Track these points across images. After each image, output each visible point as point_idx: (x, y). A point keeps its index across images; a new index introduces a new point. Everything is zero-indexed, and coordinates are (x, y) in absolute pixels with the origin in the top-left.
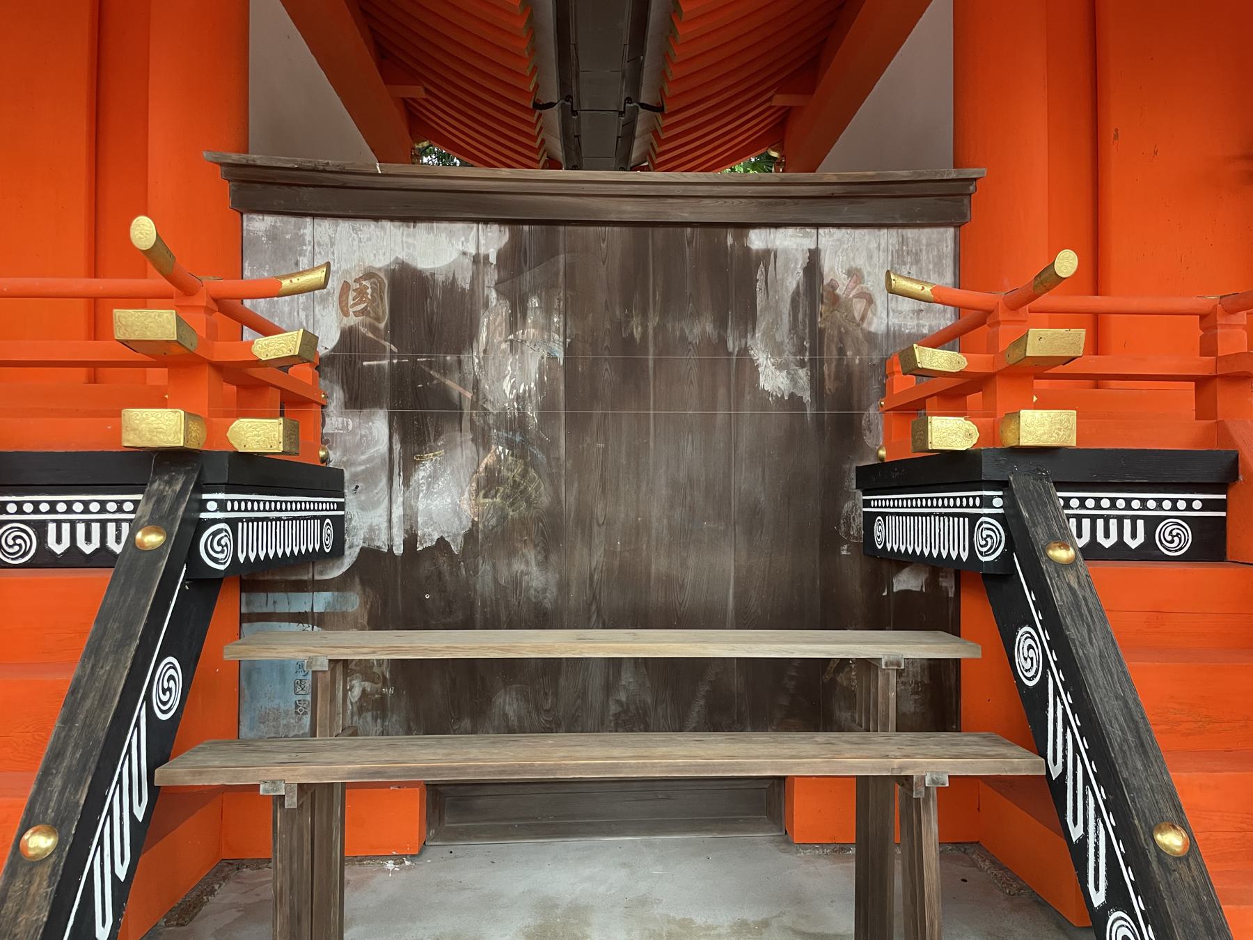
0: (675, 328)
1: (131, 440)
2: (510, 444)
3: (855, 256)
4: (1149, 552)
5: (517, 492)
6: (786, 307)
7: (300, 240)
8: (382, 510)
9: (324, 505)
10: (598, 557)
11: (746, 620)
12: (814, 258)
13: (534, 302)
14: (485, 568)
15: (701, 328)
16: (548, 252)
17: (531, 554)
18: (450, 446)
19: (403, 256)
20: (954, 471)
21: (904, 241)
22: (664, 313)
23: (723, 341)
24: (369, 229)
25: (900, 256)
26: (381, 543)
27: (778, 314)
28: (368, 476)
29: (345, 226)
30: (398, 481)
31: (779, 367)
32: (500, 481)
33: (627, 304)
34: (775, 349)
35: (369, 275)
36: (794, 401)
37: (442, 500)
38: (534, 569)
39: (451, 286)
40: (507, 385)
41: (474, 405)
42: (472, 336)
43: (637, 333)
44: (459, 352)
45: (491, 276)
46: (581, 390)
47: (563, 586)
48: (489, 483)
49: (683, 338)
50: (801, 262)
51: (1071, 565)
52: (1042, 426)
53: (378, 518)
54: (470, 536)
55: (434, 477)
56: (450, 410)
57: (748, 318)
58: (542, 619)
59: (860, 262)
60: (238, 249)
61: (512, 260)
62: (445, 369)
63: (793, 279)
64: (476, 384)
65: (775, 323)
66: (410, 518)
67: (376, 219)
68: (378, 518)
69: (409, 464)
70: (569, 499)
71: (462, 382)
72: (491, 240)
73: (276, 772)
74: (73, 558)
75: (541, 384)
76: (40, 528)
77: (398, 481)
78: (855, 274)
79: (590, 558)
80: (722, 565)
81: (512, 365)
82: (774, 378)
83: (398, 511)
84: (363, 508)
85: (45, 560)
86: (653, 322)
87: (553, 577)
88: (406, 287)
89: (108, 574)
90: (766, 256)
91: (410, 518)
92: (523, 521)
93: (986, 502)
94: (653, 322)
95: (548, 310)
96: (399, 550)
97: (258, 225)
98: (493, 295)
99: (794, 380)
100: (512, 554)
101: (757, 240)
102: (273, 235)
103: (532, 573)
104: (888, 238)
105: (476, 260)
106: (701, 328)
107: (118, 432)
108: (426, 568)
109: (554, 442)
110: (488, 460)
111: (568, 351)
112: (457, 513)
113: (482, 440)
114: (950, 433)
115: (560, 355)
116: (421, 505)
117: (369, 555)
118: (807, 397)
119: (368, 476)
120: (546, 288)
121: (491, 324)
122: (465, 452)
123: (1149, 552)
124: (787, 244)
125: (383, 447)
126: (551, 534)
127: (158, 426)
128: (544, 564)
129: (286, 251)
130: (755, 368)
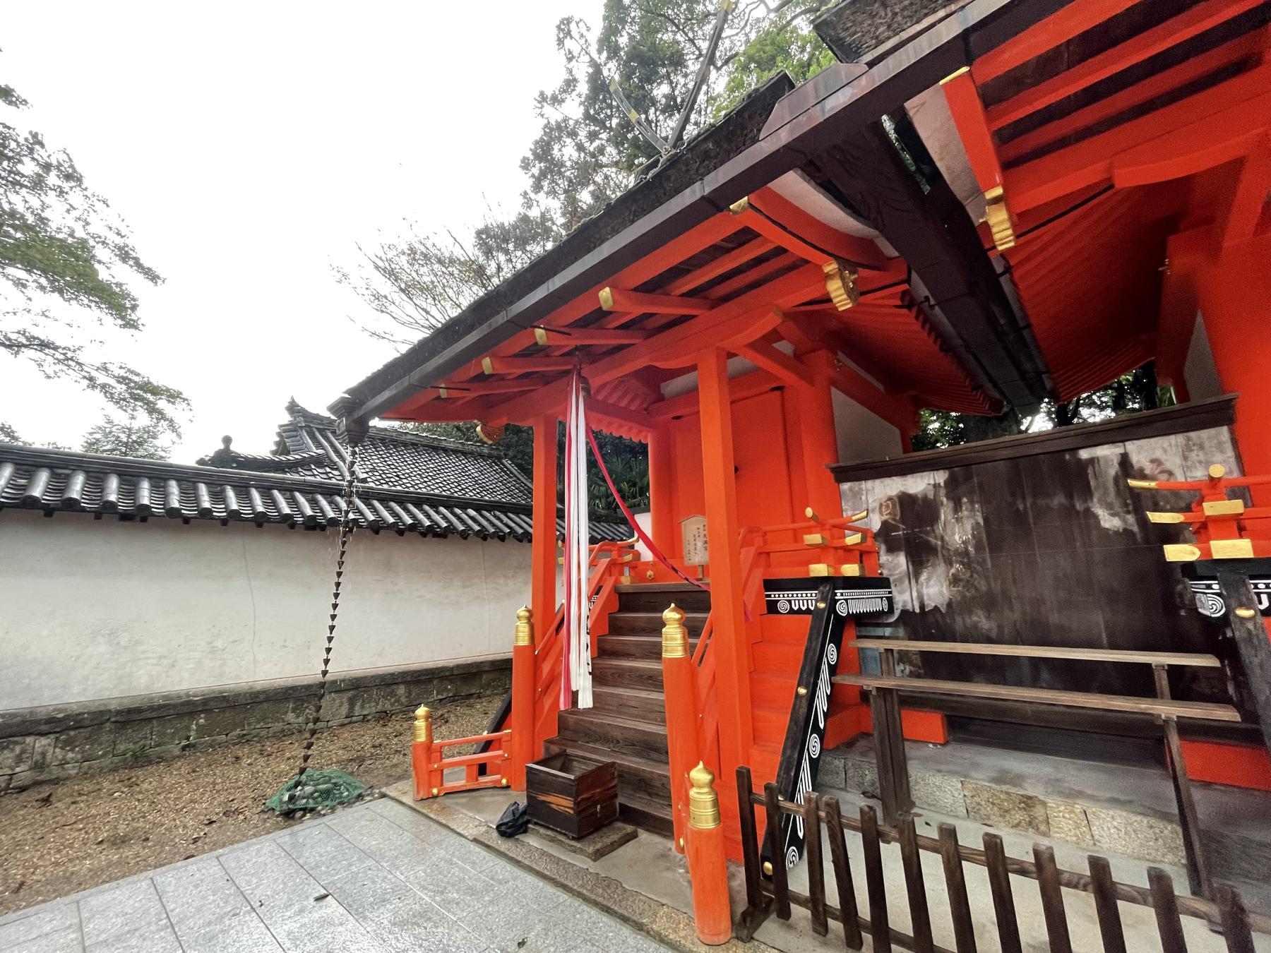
0: (1042, 502)
1: (812, 575)
2: (962, 563)
5: (969, 584)
6: (1111, 484)
7: (861, 489)
8: (908, 593)
9: (882, 592)
10: (1017, 615)
11: (1114, 646)
13: (965, 500)
14: (958, 619)
15: (1058, 500)
16: (968, 478)
17: (980, 613)
18: (934, 565)
19: (902, 489)
21: (1189, 439)
22: (1035, 496)
23: (1073, 506)
24: (887, 481)
25: (1188, 448)
26: (909, 607)
27: (1106, 488)
28: (900, 580)
29: (877, 482)
30: (913, 582)
31: (1113, 515)
32: (961, 580)
33: (1013, 494)
34: (1109, 507)
35: (890, 499)
36: (1127, 532)
37: (934, 589)
38: (984, 620)
39: (925, 498)
40: (957, 537)
41: (943, 547)
42: (937, 518)
43: (1021, 507)
44: (932, 526)
45: (942, 492)
46: (991, 538)
47: (1000, 627)
48: (955, 581)
49: (1048, 507)
51: (1252, 618)
53: (906, 597)
54: (949, 605)
55: (928, 579)
57: (1087, 493)
58: (989, 640)
59: (1158, 454)
60: (839, 496)
61: (951, 484)
62: (927, 533)
63: (1113, 470)
64: (942, 539)
65: (1106, 493)
66: (920, 597)
67: (890, 476)
68: (906, 597)
69: (917, 575)
70: (997, 588)
71: (936, 538)
72: (941, 477)
73: (868, 682)
74: (800, 611)
75: (973, 535)
76: (790, 602)
77: (913, 582)
79: (1013, 616)
80: (1098, 619)
81: (958, 529)
83: (915, 594)
84: (901, 593)
85: (792, 611)
86: (1029, 501)
87: (994, 625)
88: (905, 501)
89: (810, 617)
90: (1092, 461)
91: (920, 597)
92: (974, 598)
93: (1209, 587)
94: (1029, 501)
95: (972, 502)
96: (917, 610)
97: (845, 486)
98: (945, 500)
99: (1124, 521)
100: (970, 613)
101: (1084, 454)
102: (851, 489)
103: (982, 621)
104: (1177, 440)
105: (935, 486)
106: (1058, 500)
107: (808, 572)
108: (931, 619)
109: (984, 561)
110: (953, 571)
111: (986, 519)
112: (941, 593)
113: (949, 563)
115: (982, 522)
116: (925, 591)
117: (905, 613)
118: (1135, 529)
119: (900, 580)
120: (969, 494)
121: (946, 512)
122: (941, 568)
124: (1108, 453)
125: (905, 567)
126: (989, 603)
128: (988, 618)
129: (856, 495)
130: (1096, 517)
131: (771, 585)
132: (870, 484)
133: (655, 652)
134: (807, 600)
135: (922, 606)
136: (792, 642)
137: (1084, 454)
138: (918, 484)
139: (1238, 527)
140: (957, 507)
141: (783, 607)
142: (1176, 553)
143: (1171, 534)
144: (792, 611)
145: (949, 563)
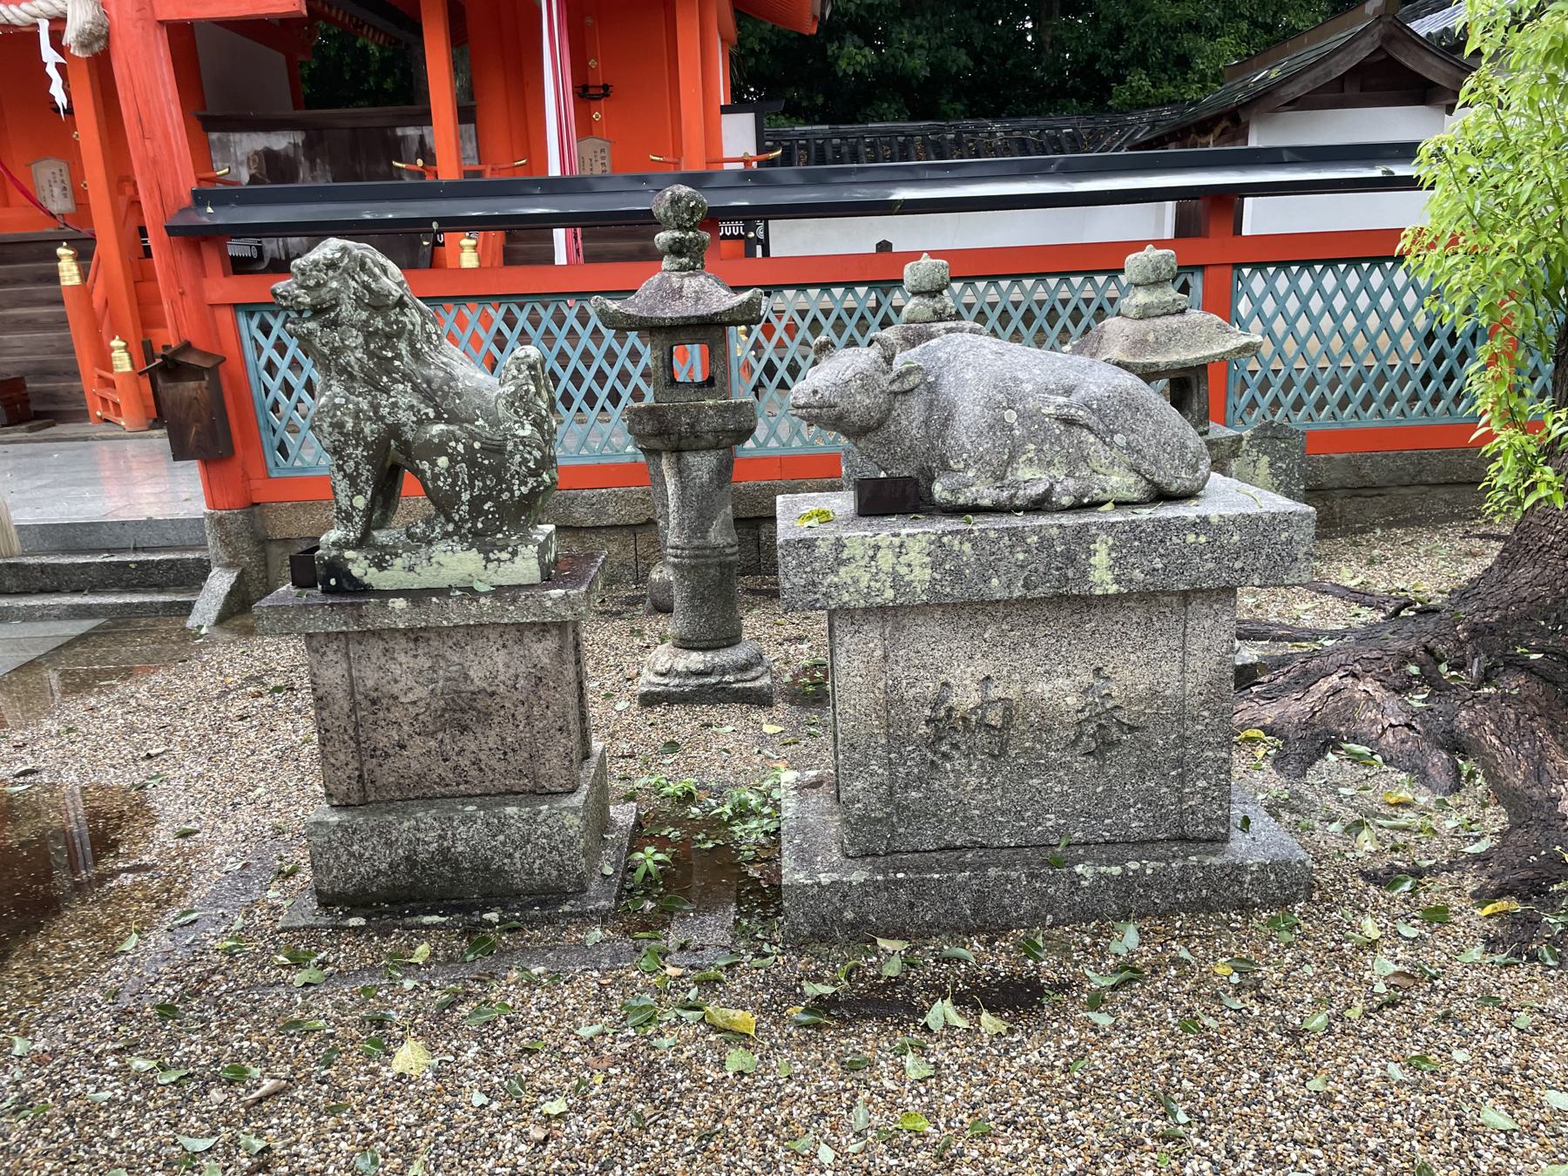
12: (422, 137)
24: (254, 135)
35: (256, 153)
45: (301, 151)
50: (417, 140)
61: (309, 145)
72: (298, 137)
88: (269, 156)
90: (404, 137)
97: (214, 136)
101: (399, 132)
102: (219, 139)
117: (273, 260)
129: (225, 146)
133: (54, 278)
137: (399, 132)
138: (280, 142)
140: (313, 168)
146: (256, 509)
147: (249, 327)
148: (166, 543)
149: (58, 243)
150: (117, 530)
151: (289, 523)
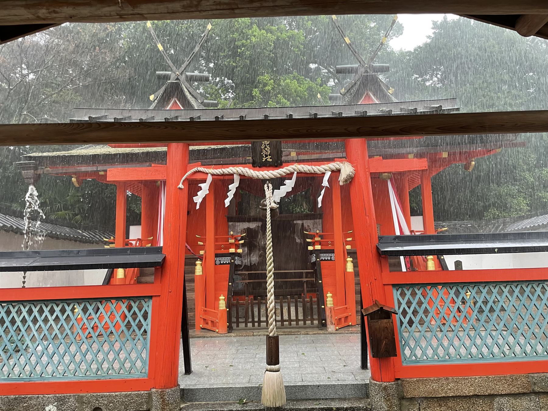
3: (307, 223)
4: (331, 260)
12: (303, 224)
18: (255, 251)
20: (312, 252)
28: (245, 256)
34: (298, 236)
35: (244, 229)
42: (258, 236)
45: (260, 228)
52: (318, 247)
55: (253, 255)
56: (255, 246)
57: (294, 233)
60: (228, 227)
63: (300, 227)
66: (250, 260)
68: (246, 261)
69: (250, 254)
74: (223, 264)
78: (308, 226)
82: (298, 241)
85: (221, 264)
88: (249, 230)
91: (250, 260)
97: (230, 223)
101: (295, 222)
102: (232, 225)
104: (312, 221)
113: (259, 250)
114: (310, 248)
119: (245, 256)
123: (331, 260)
124: (300, 222)
127: (232, 250)
129: (234, 226)
131: (217, 256)
132: (238, 224)
134: (227, 260)
135: (251, 264)
136: (226, 271)
137: (295, 222)
139: (320, 243)
141: (218, 262)
142: (310, 248)
143: (309, 244)
144: (221, 264)
145: (259, 250)
146: (399, 382)
147: (396, 294)
148: (337, 396)
149: (196, 259)
150: (315, 389)
151: (415, 389)
